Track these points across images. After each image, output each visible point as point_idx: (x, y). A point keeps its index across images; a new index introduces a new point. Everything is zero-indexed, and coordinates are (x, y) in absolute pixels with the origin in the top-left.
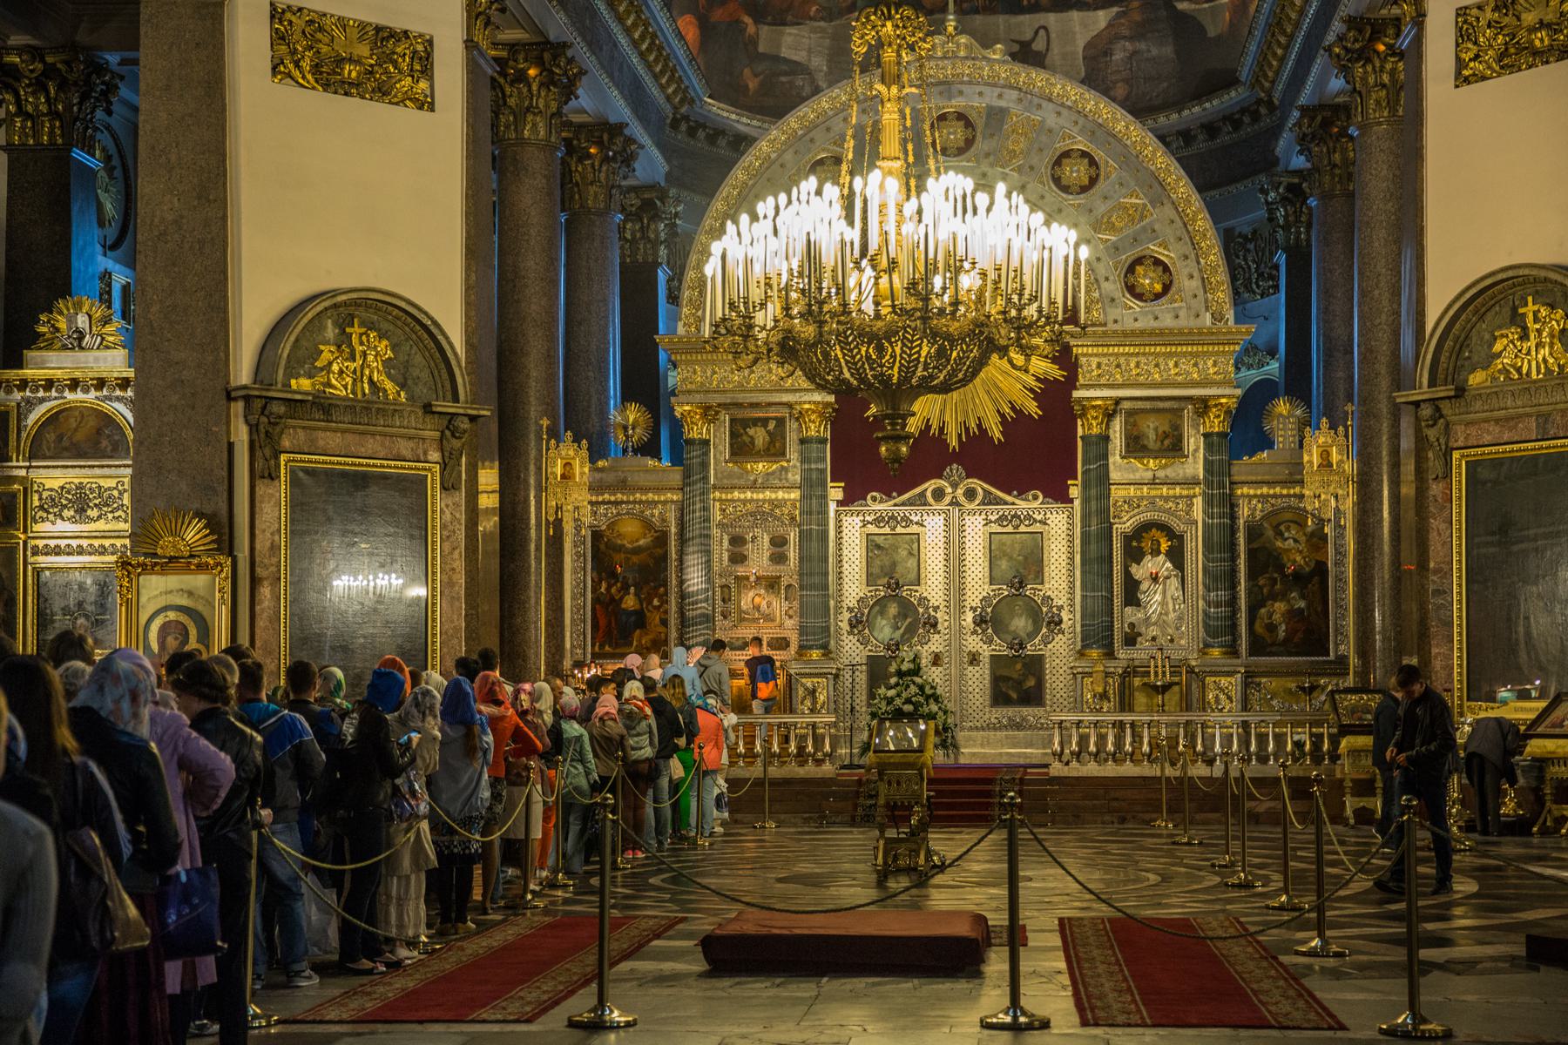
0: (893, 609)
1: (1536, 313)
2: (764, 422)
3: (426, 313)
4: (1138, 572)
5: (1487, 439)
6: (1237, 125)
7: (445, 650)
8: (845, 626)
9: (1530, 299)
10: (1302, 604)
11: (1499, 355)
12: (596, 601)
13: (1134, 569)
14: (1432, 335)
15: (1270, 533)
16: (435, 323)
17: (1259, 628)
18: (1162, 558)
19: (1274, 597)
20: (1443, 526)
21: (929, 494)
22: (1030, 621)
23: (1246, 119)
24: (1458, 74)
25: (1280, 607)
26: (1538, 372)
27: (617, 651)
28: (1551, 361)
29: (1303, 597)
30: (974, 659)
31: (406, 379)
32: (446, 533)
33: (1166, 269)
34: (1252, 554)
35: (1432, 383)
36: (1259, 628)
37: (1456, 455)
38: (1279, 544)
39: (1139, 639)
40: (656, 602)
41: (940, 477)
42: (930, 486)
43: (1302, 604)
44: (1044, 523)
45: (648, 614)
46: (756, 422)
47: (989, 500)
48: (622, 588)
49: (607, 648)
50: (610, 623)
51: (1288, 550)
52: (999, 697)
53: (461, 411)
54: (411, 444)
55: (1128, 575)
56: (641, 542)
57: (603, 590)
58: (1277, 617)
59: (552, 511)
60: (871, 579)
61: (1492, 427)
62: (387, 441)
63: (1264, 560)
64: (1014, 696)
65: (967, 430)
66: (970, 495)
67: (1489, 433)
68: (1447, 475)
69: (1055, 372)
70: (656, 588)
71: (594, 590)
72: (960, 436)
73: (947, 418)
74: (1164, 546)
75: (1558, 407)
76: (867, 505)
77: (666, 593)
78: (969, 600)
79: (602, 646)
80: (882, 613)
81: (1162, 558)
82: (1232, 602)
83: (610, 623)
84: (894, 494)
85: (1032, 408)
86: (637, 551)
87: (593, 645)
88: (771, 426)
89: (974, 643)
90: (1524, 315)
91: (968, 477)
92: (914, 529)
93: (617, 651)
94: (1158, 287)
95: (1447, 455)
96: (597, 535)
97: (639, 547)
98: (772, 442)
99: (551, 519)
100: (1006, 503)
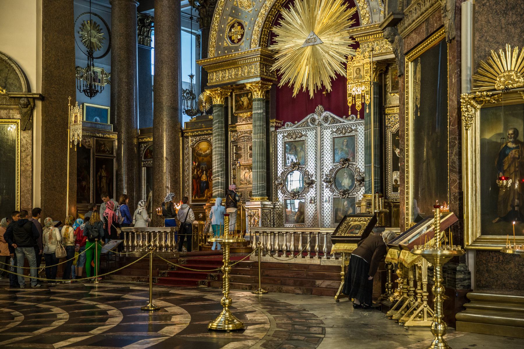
7: (23, 199)
22: (351, 180)
27: (200, 199)
31: (6, 84)
32: (23, 149)
44: (356, 130)
45: (210, 183)
47: (334, 121)
48: (201, 172)
49: (197, 198)
50: (198, 187)
53: (24, 96)
54: (5, 111)
55: (394, 154)
57: (195, 173)
65: (317, 87)
66: (326, 119)
71: (193, 173)
72: (314, 90)
76: (285, 128)
78: (325, 171)
79: (195, 197)
83: (198, 187)
84: (296, 122)
87: (192, 196)
91: (325, 110)
92: (303, 138)
93: (200, 199)
97: (207, 154)
99: (71, 141)
100: (341, 122)
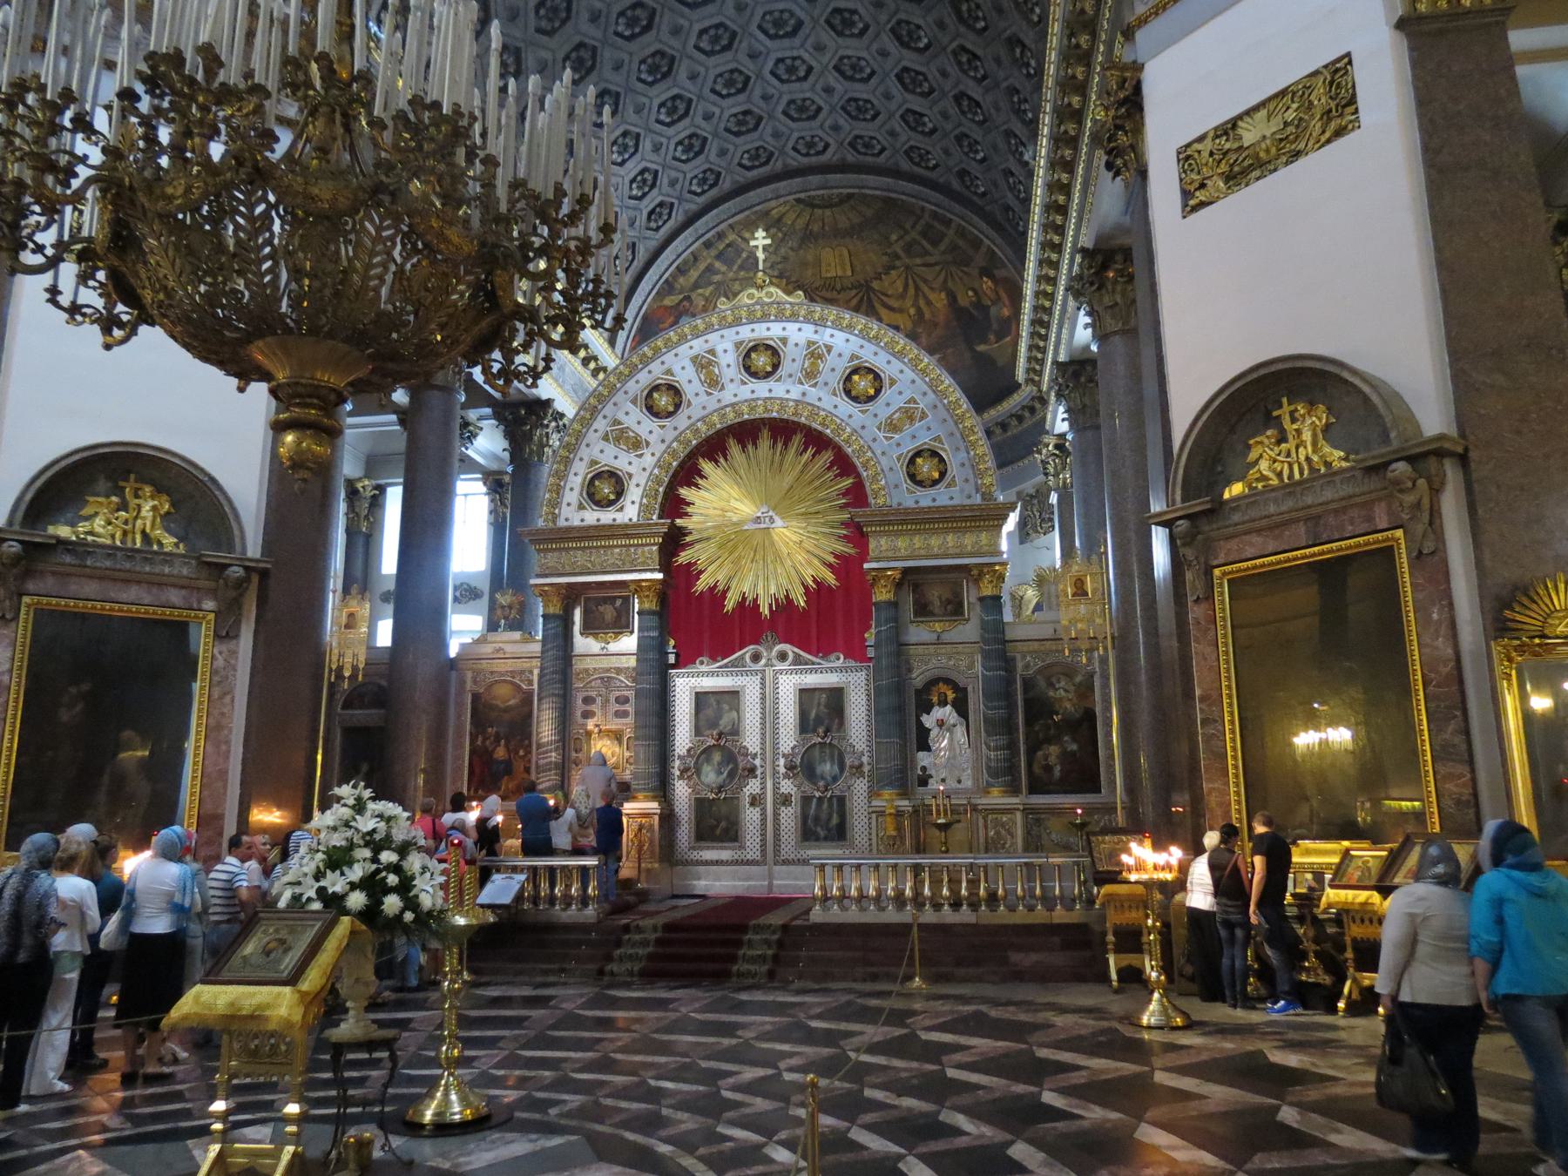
0: (717, 757)
1: (1292, 413)
2: (613, 600)
3: (202, 470)
4: (928, 721)
5: (1249, 552)
6: (1020, 419)
7: (206, 793)
8: (677, 773)
9: (1285, 400)
10: (1074, 747)
11: (1256, 462)
12: (472, 753)
13: (928, 721)
14: (1180, 455)
15: (1042, 683)
16: (213, 480)
17: (1037, 770)
18: (949, 708)
19: (1048, 741)
20: (1209, 650)
21: (747, 657)
23: (1027, 414)
24: (1185, 205)
25: (1054, 750)
26: (1301, 473)
28: (1315, 458)
29: (1074, 740)
30: (786, 800)
32: (217, 678)
33: (942, 460)
34: (1027, 702)
35: (1184, 501)
36: (1037, 770)
37: (1217, 572)
38: (1051, 693)
39: (931, 781)
40: (521, 753)
41: (757, 642)
42: (748, 651)
43: (1074, 747)
46: (605, 600)
51: (1061, 699)
52: (808, 833)
55: (920, 725)
56: (512, 702)
58: (1053, 760)
59: (334, 658)
60: (698, 731)
61: (1256, 539)
62: (155, 590)
64: (822, 833)
66: (783, 657)
67: (1252, 545)
68: (1209, 597)
69: (849, 549)
70: (522, 741)
73: (760, 592)
74: (951, 695)
75: (1331, 506)
77: (530, 745)
80: (708, 760)
81: (949, 708)
82: (1012, 746)
85: (831, 579)
86: (507, 710)
88: (618, 602)
89: (787, 786)
90: (1279, 417)
94: (936, 475)
95: (1208, 572)
96: (476, 697)
98: (619, 616)
99: (334, 667)
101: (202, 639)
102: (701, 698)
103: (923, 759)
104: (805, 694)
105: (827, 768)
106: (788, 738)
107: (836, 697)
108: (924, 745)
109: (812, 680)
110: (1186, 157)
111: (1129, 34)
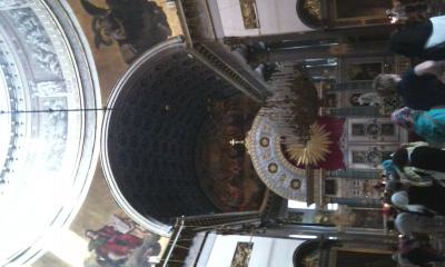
63: (359, 77)
89: (379, 138)
101: (341, 249)
102: (355, 161)
103: (372, 104)
104: (354, 133)
105: (374, 129)
106: (366, 138)
107: (354, 126)
108: (368, 104)
109: (350, 131)
110: (247, 27)
111: (216, 39)
